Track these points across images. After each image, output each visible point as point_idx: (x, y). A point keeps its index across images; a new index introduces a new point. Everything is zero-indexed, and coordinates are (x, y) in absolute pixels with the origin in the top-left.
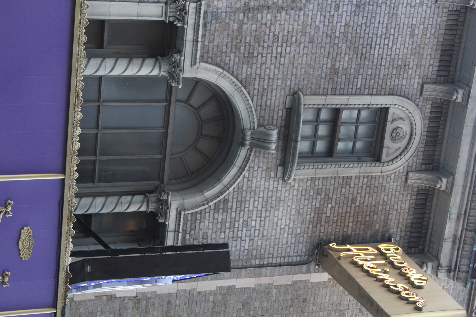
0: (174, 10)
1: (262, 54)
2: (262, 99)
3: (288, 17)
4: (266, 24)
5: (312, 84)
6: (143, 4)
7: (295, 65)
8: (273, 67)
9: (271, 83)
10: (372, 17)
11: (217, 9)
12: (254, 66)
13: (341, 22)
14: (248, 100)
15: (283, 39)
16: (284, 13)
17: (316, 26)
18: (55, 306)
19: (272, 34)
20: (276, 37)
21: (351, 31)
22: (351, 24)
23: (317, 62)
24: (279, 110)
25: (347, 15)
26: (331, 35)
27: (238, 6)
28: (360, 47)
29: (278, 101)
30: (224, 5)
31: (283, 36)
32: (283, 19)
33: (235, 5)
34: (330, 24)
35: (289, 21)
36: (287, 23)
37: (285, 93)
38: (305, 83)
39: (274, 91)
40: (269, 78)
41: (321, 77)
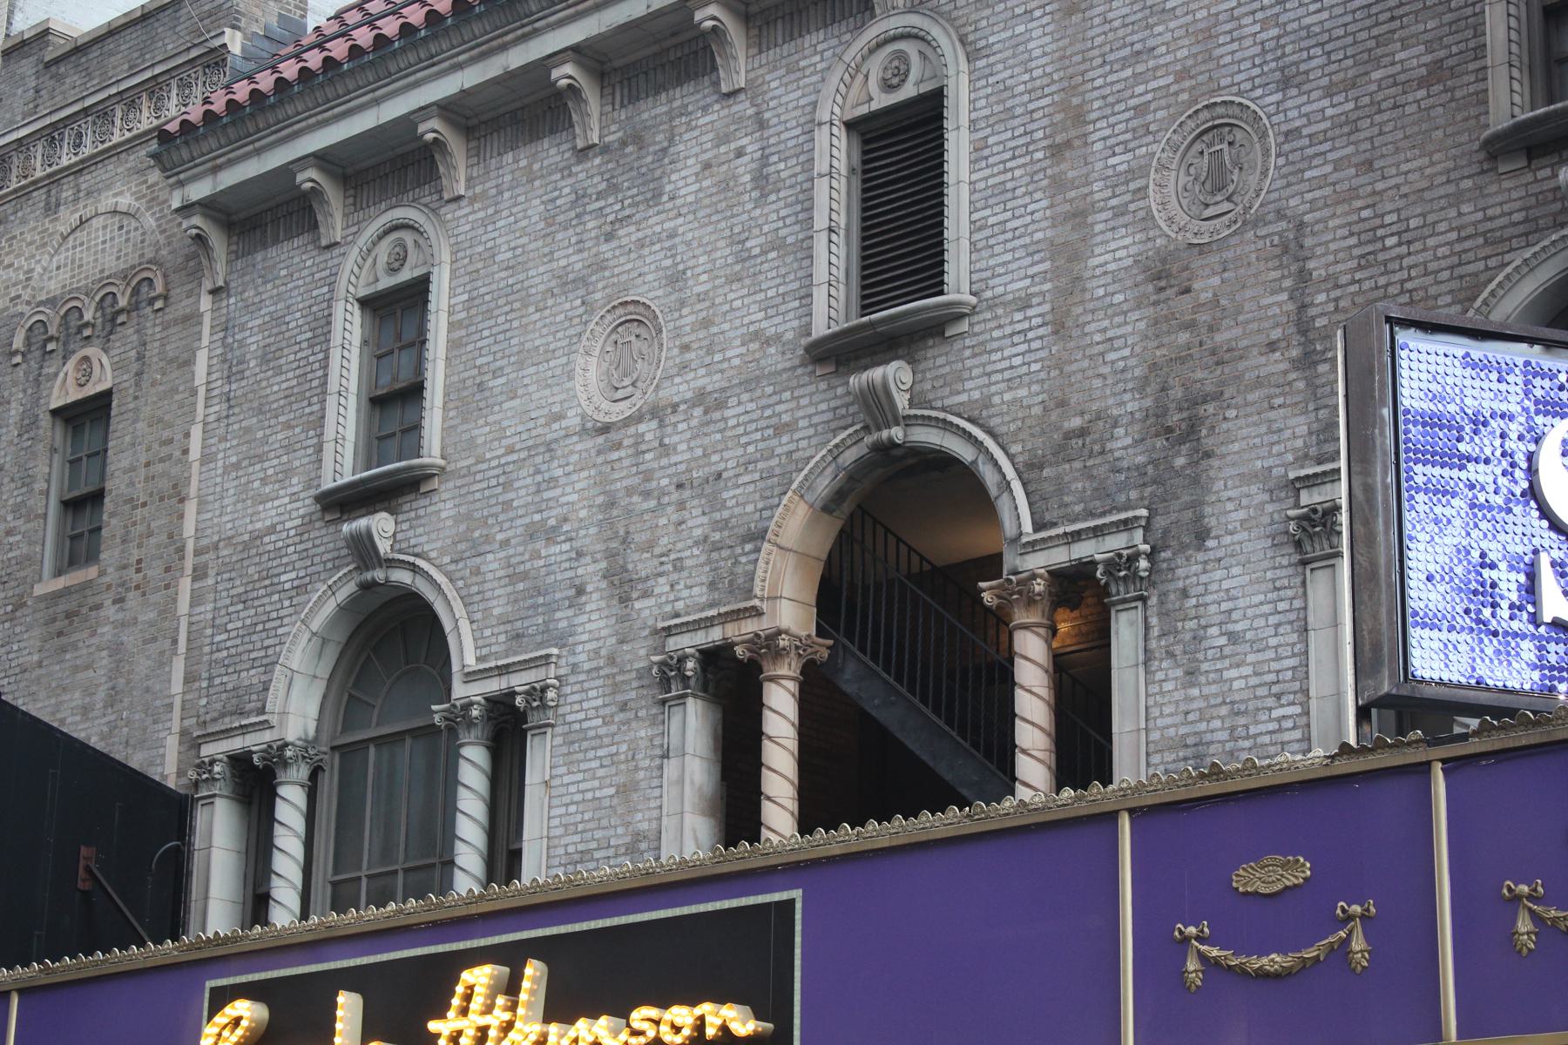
0: (1316, 539)
1: (1403, 282)
2: (1509, 239)
3: (1319, 250)
4: (1336, 300)
5: (1466, 119)
6: (1311, 619)
7: (1424, 184)
8: (1431, 242)
9: (1470, 230)
10: (1309, 37)
11: (1310, 433)
12: (1432, 291)
13: (1323, 110)
14: (1508, 277)
15: (1369, 242)
16: (1311, 265)
17: (1335, 170)
18: (1428, 764)
19: (1358, 276)
20: (1363, 262)
21: (1342, 75)
22: (1325, 81)
23: (1416, 129)
24: (1536, 181)
25: (1309, 102)
26: (1350, 124)
27: (1301, 385)
28: (1375, 32)
29: (1510, 193)
30: (1302, 419)
31: (1360, 244)
32: (1323, 260)
33: (1299, 392)
34: (1329, 134)
35: (1327, 243)
36: (1333, 246)
37: (1492, 183)
38: (1465, 138)
39: (1490, 212)
40: (1460, 240)
41: (1452, 100)
